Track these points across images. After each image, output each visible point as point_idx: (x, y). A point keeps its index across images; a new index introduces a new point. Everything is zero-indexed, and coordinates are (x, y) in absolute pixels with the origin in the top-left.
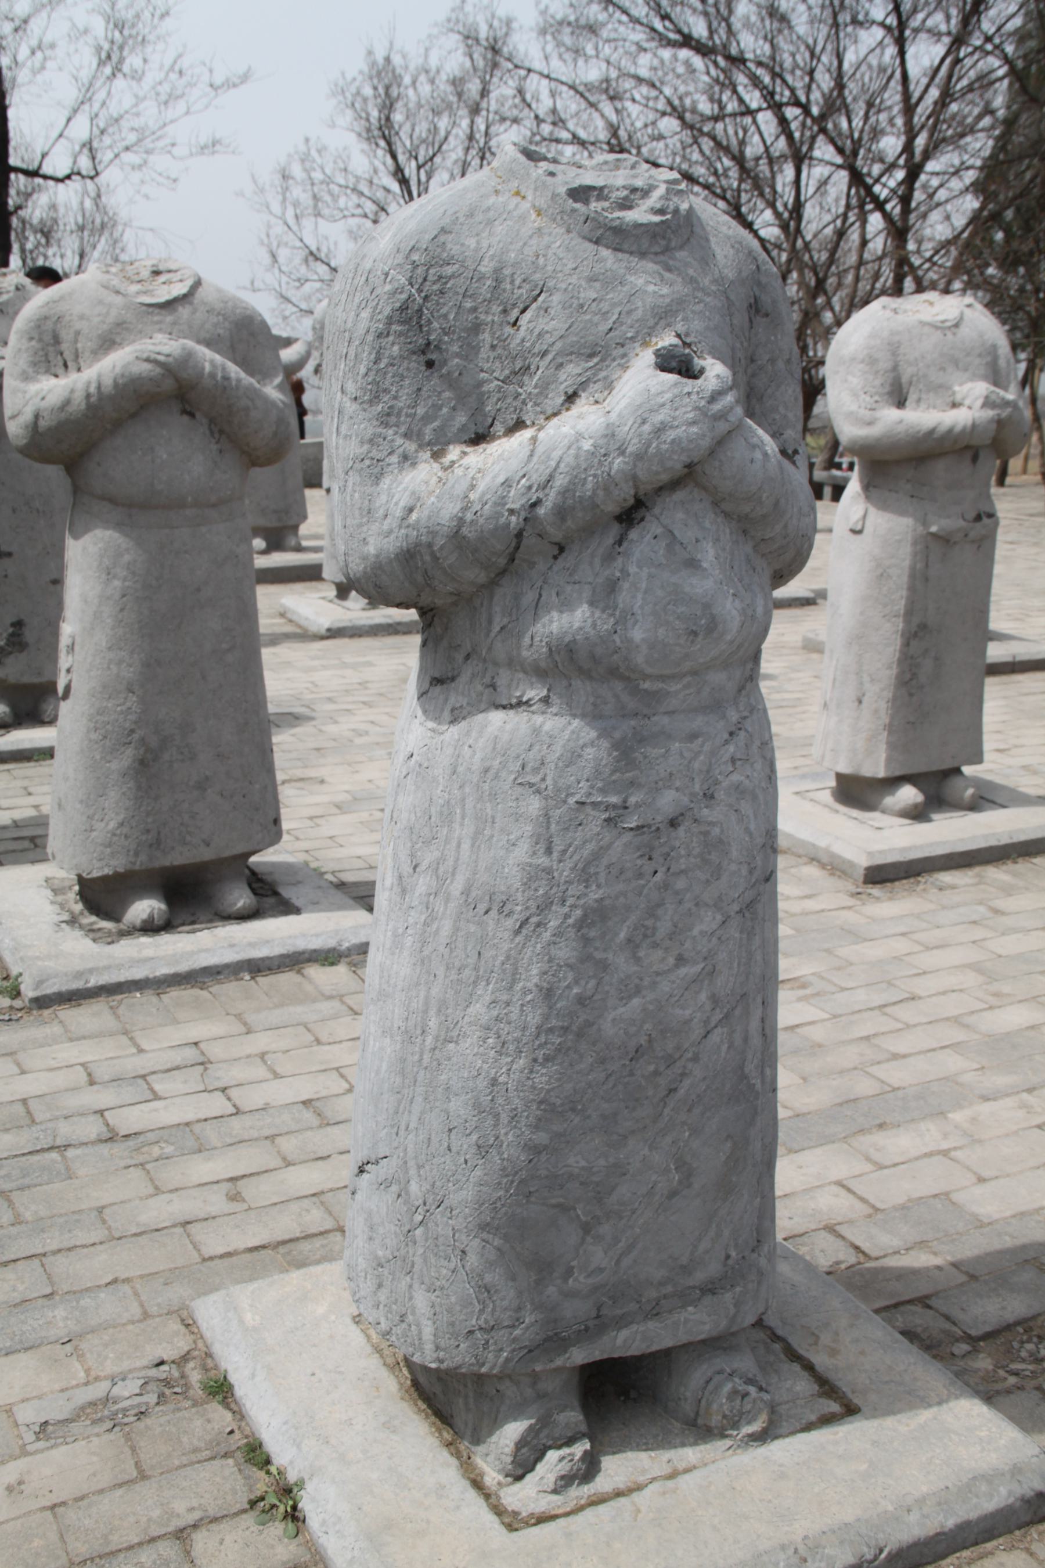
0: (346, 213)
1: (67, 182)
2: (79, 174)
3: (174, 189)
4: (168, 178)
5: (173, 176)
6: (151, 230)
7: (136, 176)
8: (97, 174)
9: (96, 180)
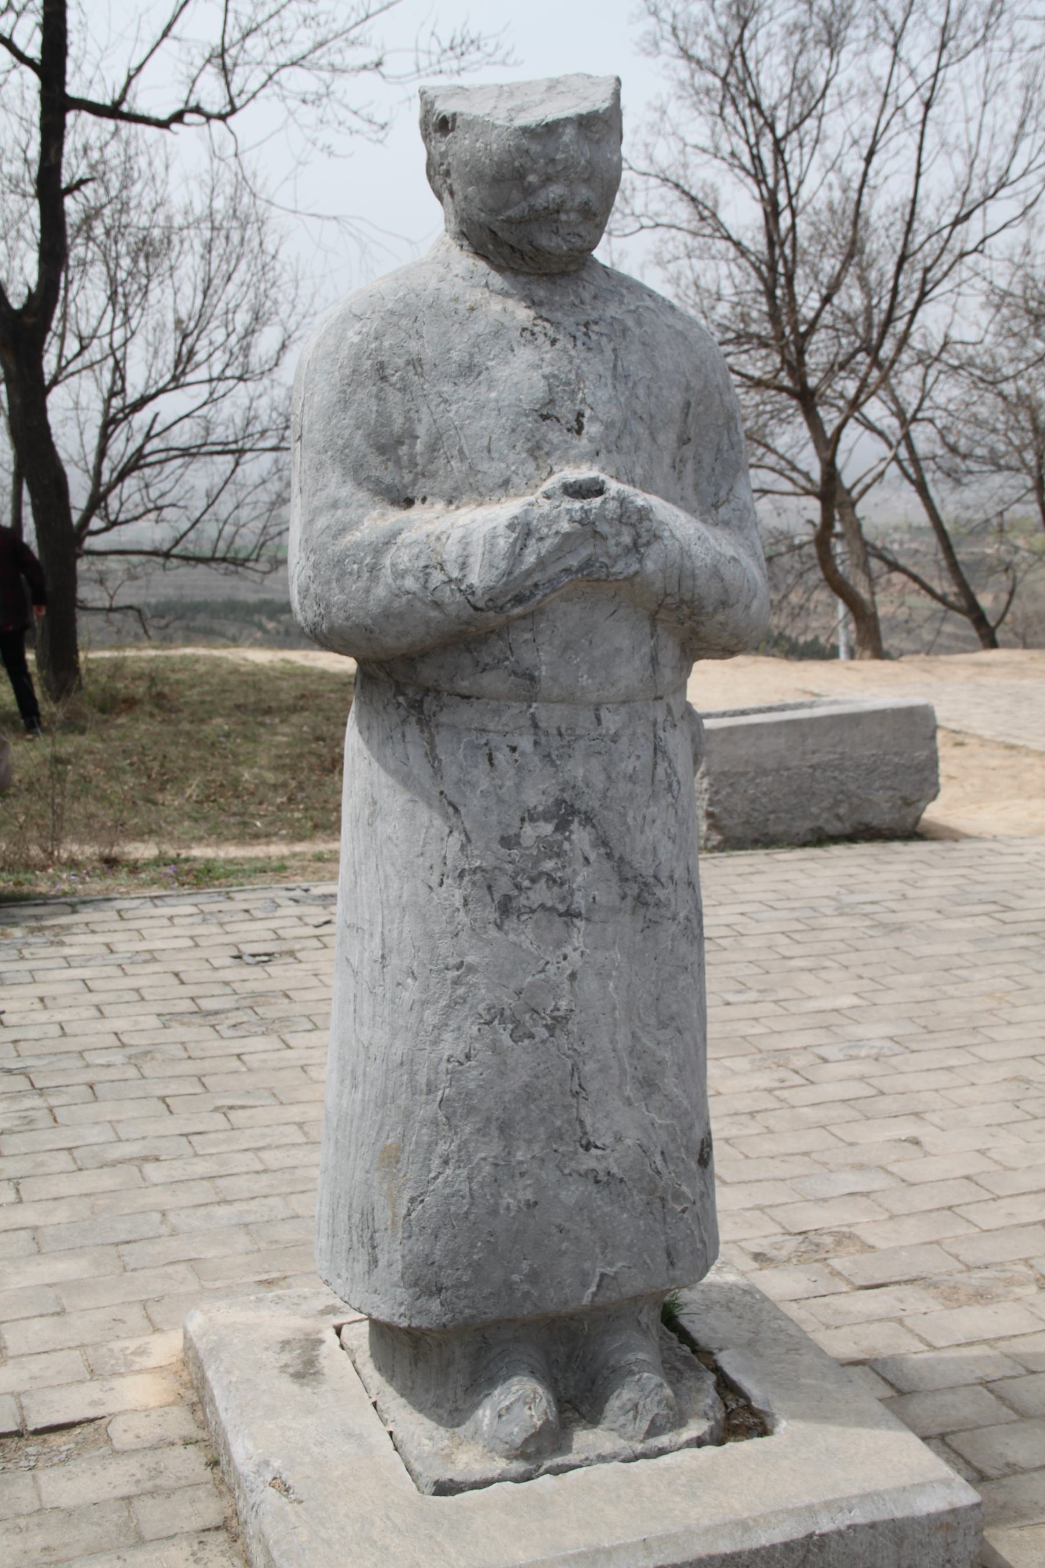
0: (645, 221)
1: (175, 127)
2: (197, 110)
3: (381, 142)
4: (370, 121)
5: (380, 119)
6: (335, 218)
7: (309, 114)
8: (234, 111)
9: (230, 120)
